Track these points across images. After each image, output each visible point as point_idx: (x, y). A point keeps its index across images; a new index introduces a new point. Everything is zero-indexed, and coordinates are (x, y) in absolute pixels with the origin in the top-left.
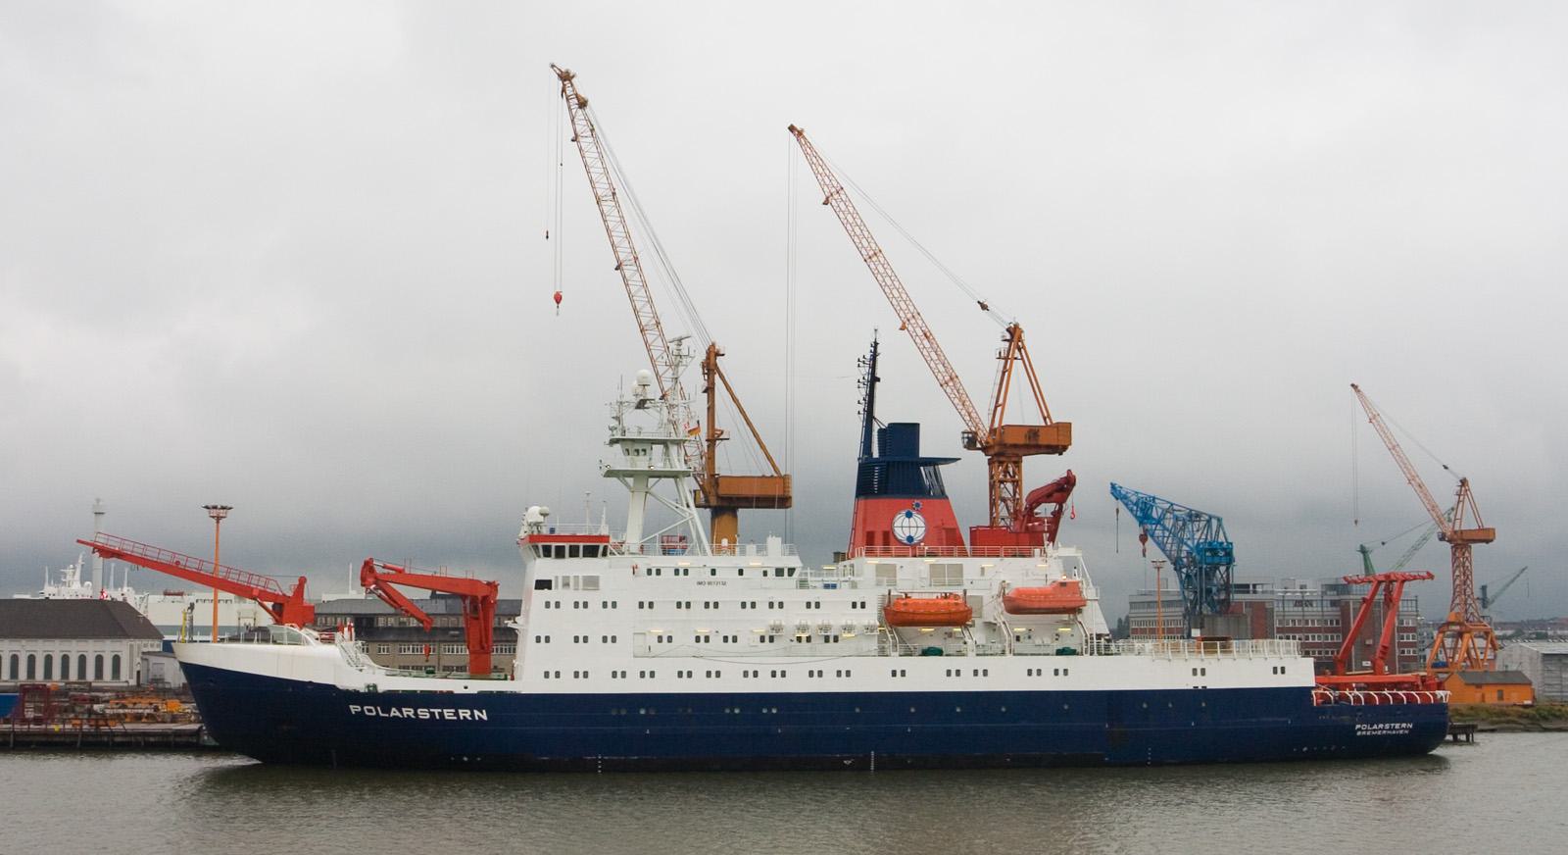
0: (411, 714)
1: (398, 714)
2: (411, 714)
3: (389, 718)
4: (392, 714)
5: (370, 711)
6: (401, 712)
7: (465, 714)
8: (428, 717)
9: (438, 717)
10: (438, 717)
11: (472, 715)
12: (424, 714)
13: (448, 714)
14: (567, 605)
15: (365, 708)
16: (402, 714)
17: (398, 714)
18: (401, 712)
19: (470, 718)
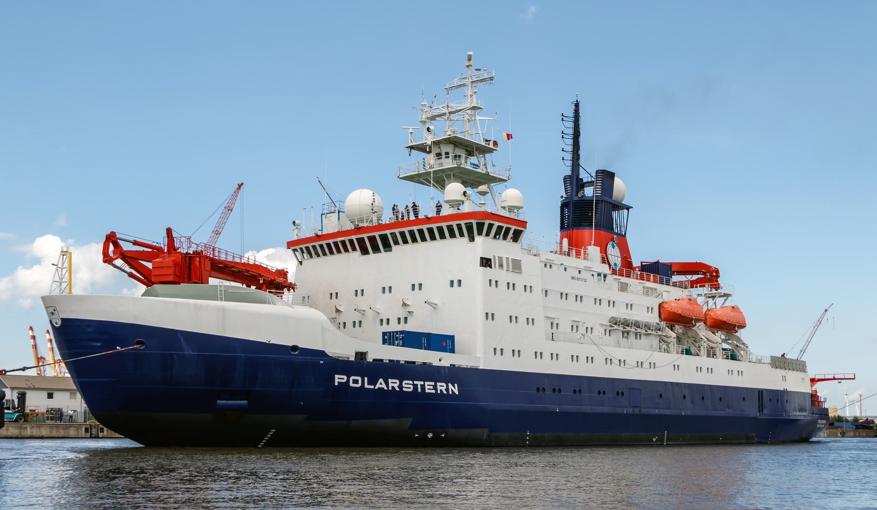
0: (396, 386)
1: (384, 386)
2: (396, 386)
3: (374, 389)
4: (378, 386)
5: (356, 382)
6: (387, 384)
7: (441, 387)
8: (411, 390)
9: (419, 391)
10: (419, 391)
11: (447, 390)
12: (408, 386)
13: (429, 387)
14: (503, 285)
15: (352, 378)
16: (388, 387)
17: (384, 386)
18: (387, 384)
19: (445, 392)
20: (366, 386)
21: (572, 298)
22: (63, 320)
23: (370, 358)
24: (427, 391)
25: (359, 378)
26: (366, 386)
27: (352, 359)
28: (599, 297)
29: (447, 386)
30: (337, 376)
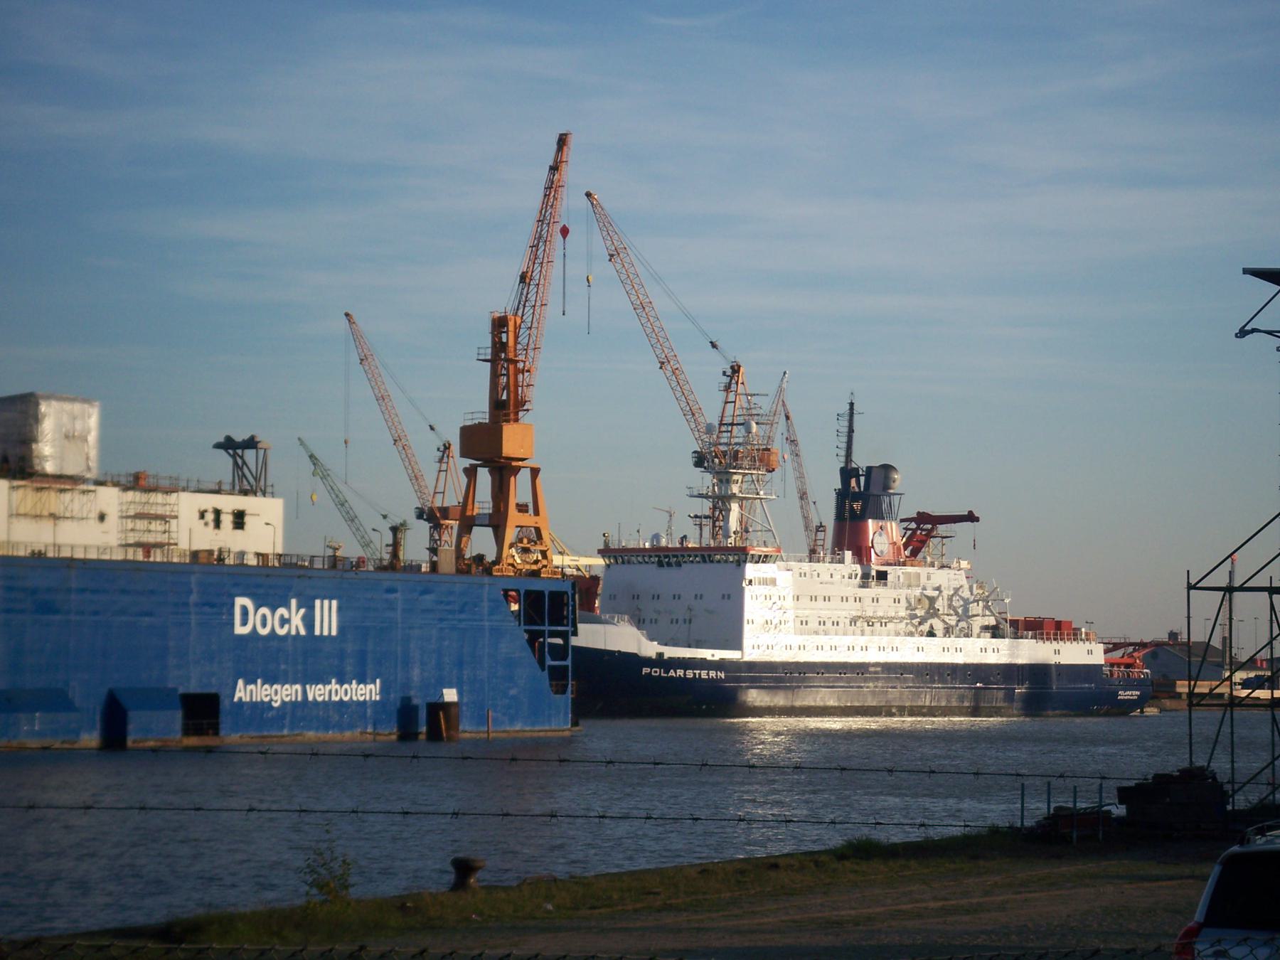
1: (674, 675)
4: (670, 674)
5: (656, 672)
6: (676, 673)
7: (713, 674)
9: (697, 676)
10: (697, 676)
11: (717, 676)
12: (690, 674)
13: (704, 674)
18: (676, 673)
20: (662, 675)
21: (820, 599)
23: (666, 657)
24: (703, 677)
25: (658, 670)
26: (662, 675)
27: (654, 657)
28: (844, 595)
30: (644, 669)
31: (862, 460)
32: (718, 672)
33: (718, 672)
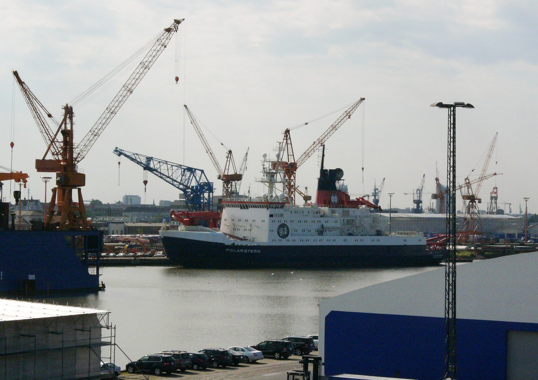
0: (242, 251)
1: (239, 251)
2: (242, 251)
5: (232, 250)
7: (255, 251)
11: (257, 252)
12: (246, 251)
13: (251, 251)
15: (231, 250)
17: (239, 251)
18: (240, 251)
20: (234, 251)
22: (164, 237)
26: (234, 251)
29: (257, 251)
30: (227, 249)
31: (327, 167)
32: (258, 251)
33: (258, 251)
